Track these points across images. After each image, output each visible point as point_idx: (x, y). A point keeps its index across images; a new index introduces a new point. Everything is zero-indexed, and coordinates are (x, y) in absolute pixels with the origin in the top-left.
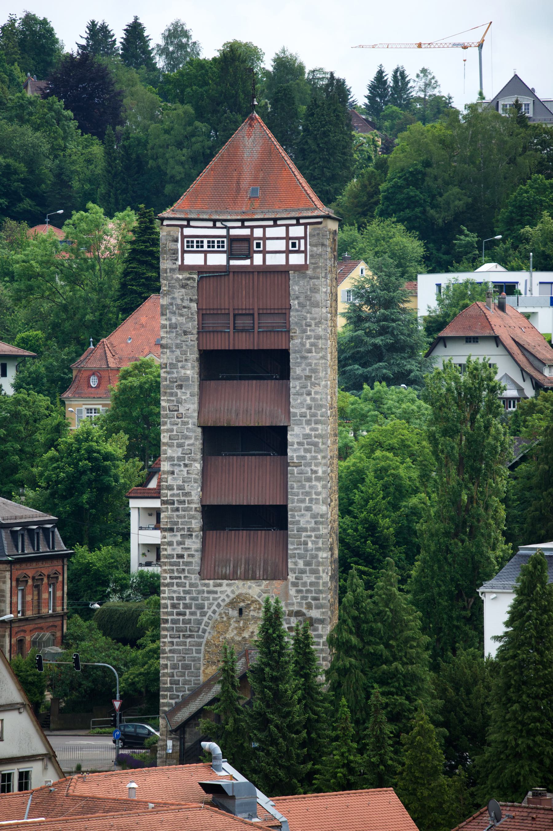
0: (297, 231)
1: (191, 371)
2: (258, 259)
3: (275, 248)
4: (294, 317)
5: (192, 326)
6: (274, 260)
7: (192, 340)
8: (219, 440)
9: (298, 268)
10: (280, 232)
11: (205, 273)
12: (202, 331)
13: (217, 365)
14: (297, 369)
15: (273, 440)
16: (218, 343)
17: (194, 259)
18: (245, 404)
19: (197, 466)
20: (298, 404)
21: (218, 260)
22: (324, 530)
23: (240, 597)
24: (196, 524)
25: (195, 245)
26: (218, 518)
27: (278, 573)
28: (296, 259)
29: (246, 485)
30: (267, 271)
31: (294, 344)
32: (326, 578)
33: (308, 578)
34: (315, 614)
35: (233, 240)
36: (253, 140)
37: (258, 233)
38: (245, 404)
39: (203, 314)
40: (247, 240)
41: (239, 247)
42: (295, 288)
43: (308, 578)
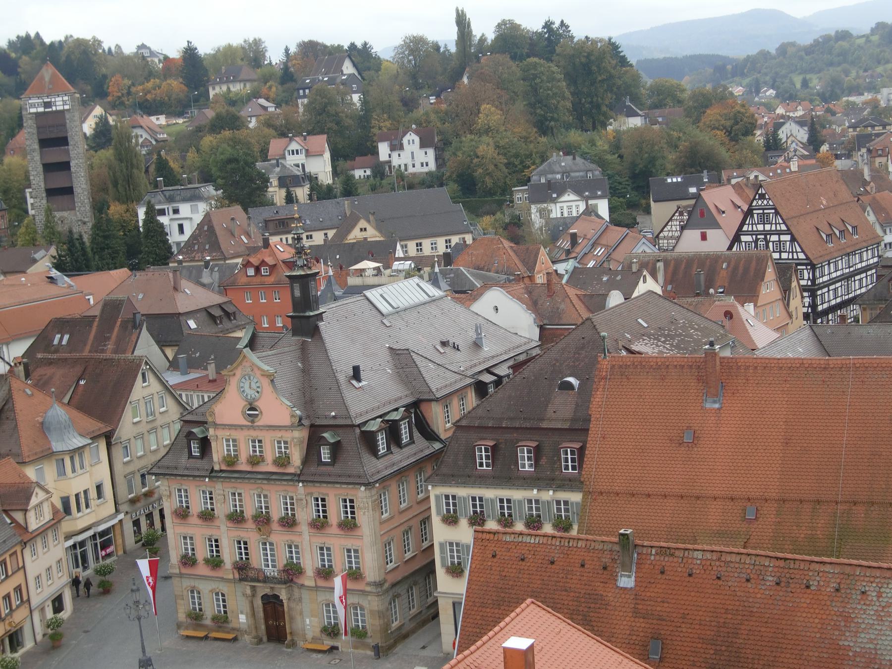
0: (66, 98)
1: (36, 146)
2: (54, 108)
3: (60, 103)
4: (68, 126)
5: (35, 131)
6: (60, 108)
7: (35, 136)
8: (48, 168)
9: (68, 110)
10: (60, 99)
11: (37, 114)
12: (39, 133)
13: (45, 143)
14: (71, 142)
15: (65, 166)
16: (44, 137)
17: (33, 110)
18: (54, 155)
19: (42, 177)
20: (73, 154)
21: (41, 110)
22: (86, 193)
23: (61, 217)
24: (44, 195)
25: (33, 106)
26: (51, 193)
27: (74, 209)
28: (67, 107)
29: (59, 181)
30: (57, 112)
31: (69, 134)
32: (88, 208)
33: (82, 209)
34: (86, 220)
35: (45, 103)
36: (48, 72)
37: (53, 100)
38: (54, 155)
39: (38, 128)
40: (50, 102)
41: (47, 105)
42: (67, 116)
43: (82, 209)
